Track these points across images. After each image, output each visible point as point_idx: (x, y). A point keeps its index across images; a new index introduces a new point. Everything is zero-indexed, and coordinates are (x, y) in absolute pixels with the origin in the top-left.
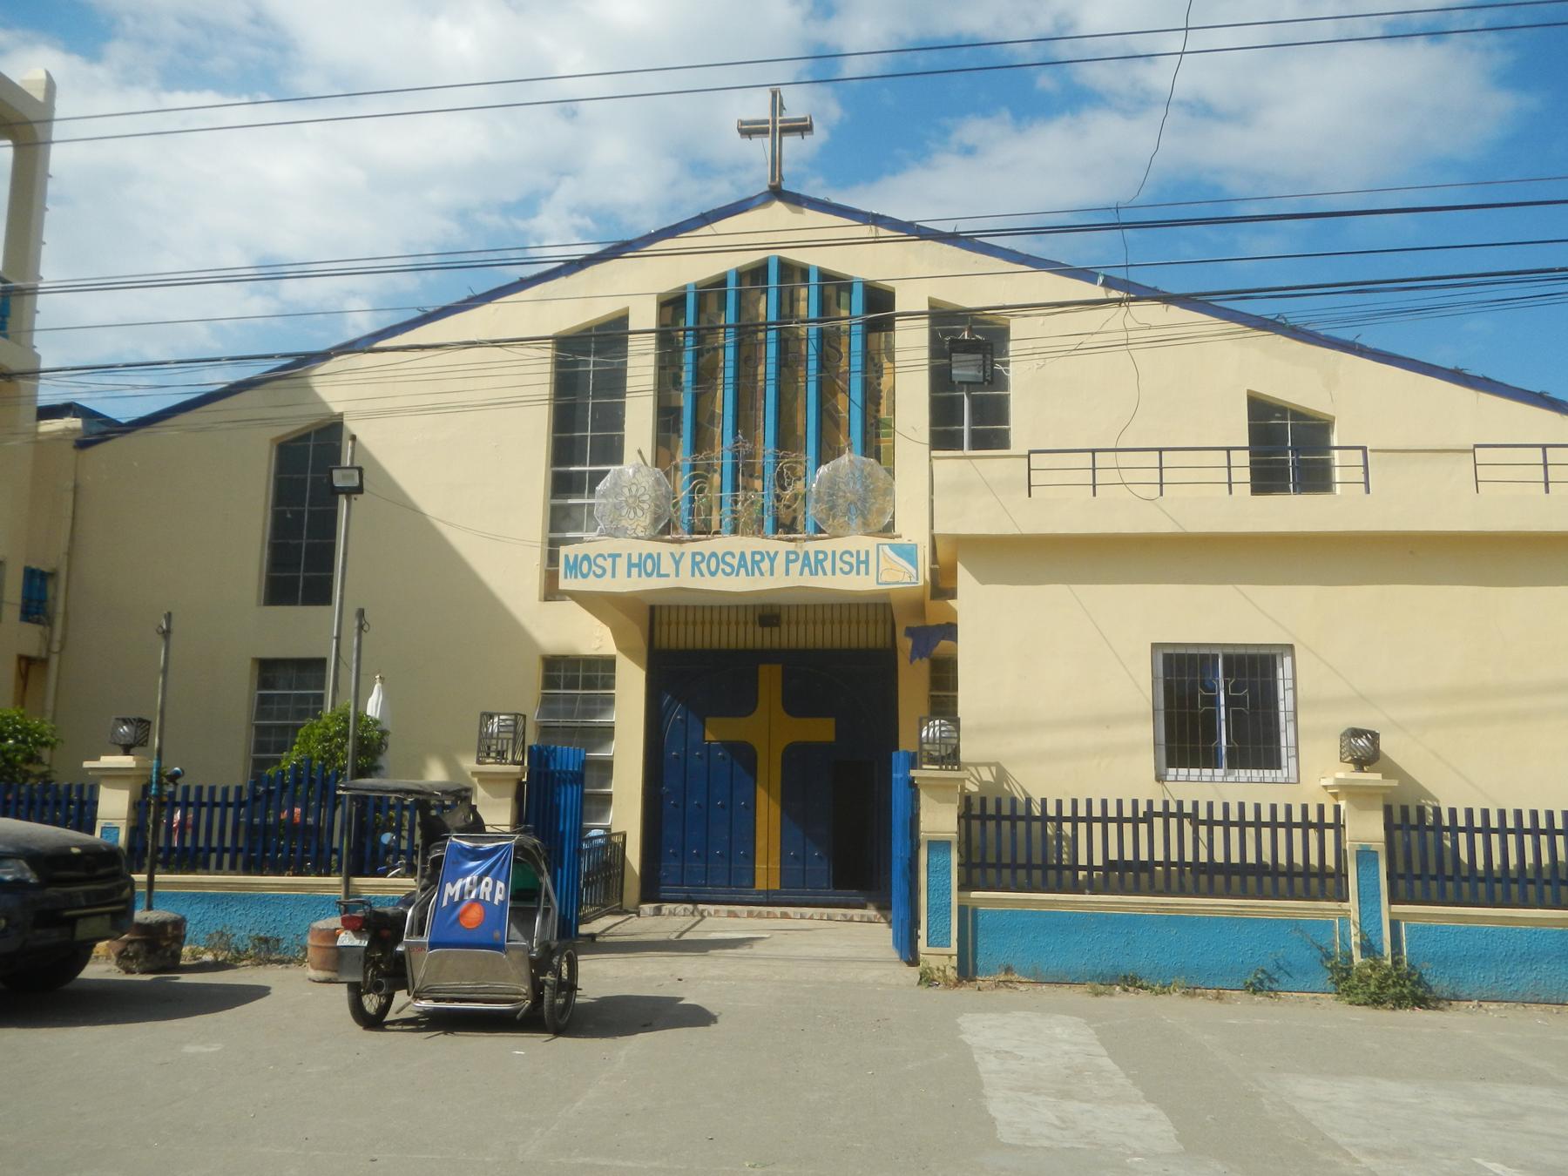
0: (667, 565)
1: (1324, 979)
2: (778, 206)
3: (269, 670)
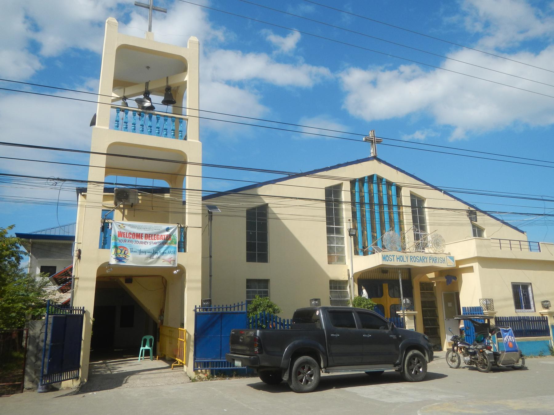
0: (405, 259)
1: (549, 353)
2: (375, 161)
3: (250, 283)
